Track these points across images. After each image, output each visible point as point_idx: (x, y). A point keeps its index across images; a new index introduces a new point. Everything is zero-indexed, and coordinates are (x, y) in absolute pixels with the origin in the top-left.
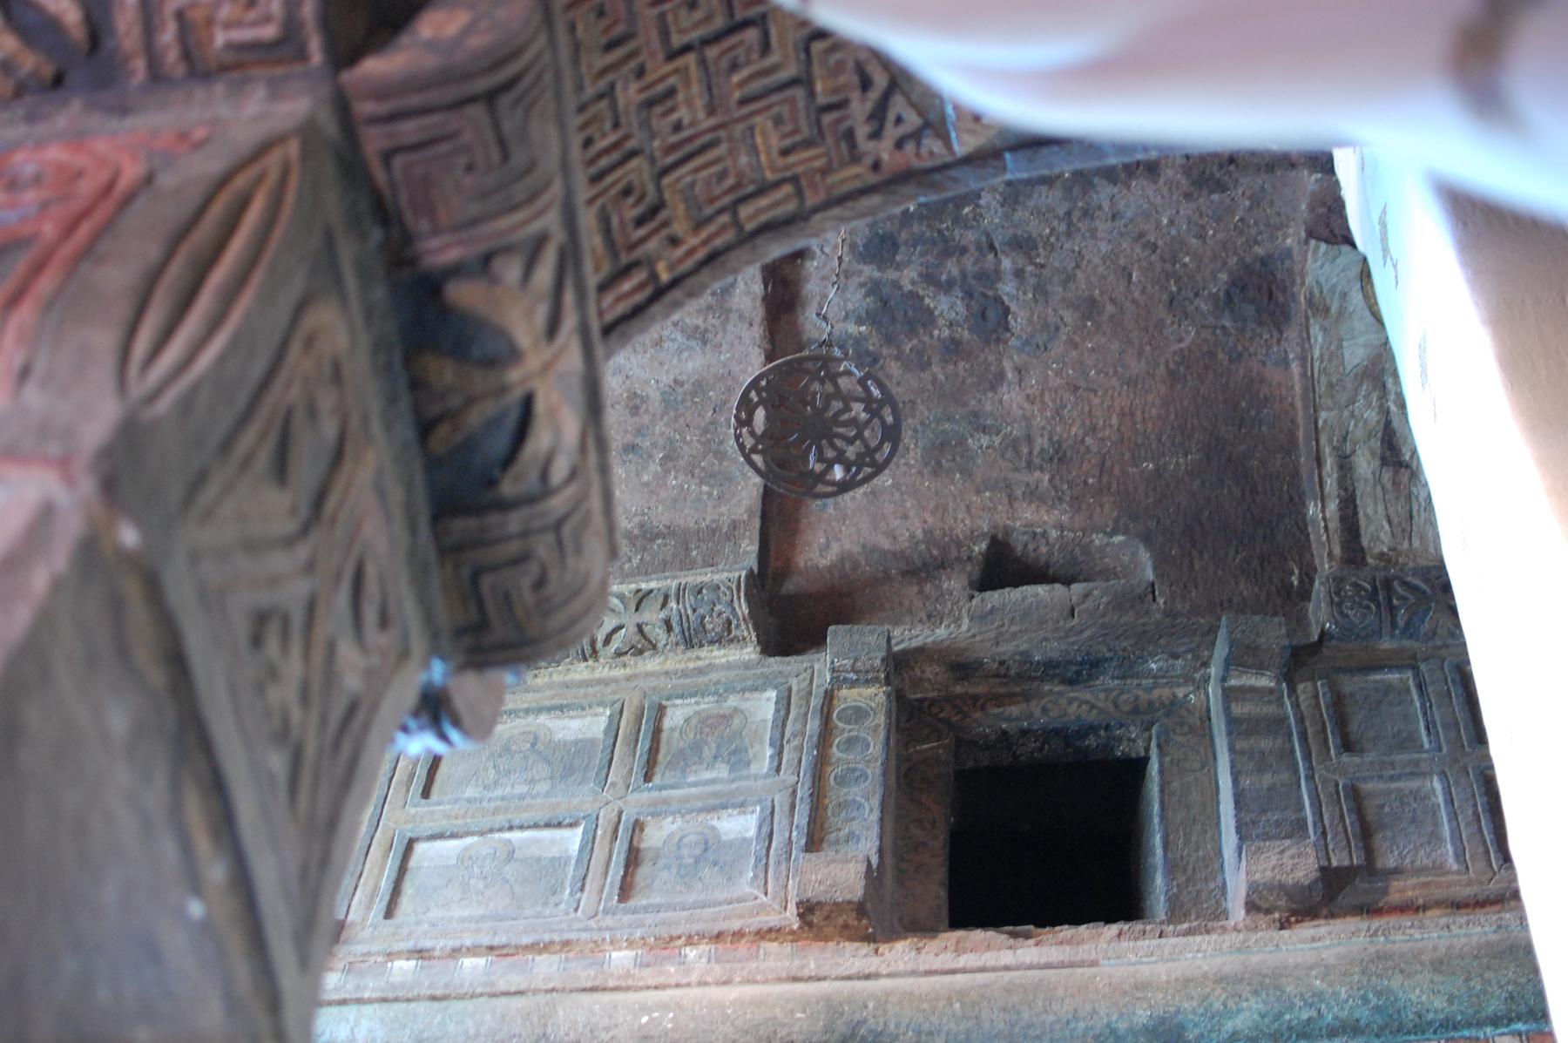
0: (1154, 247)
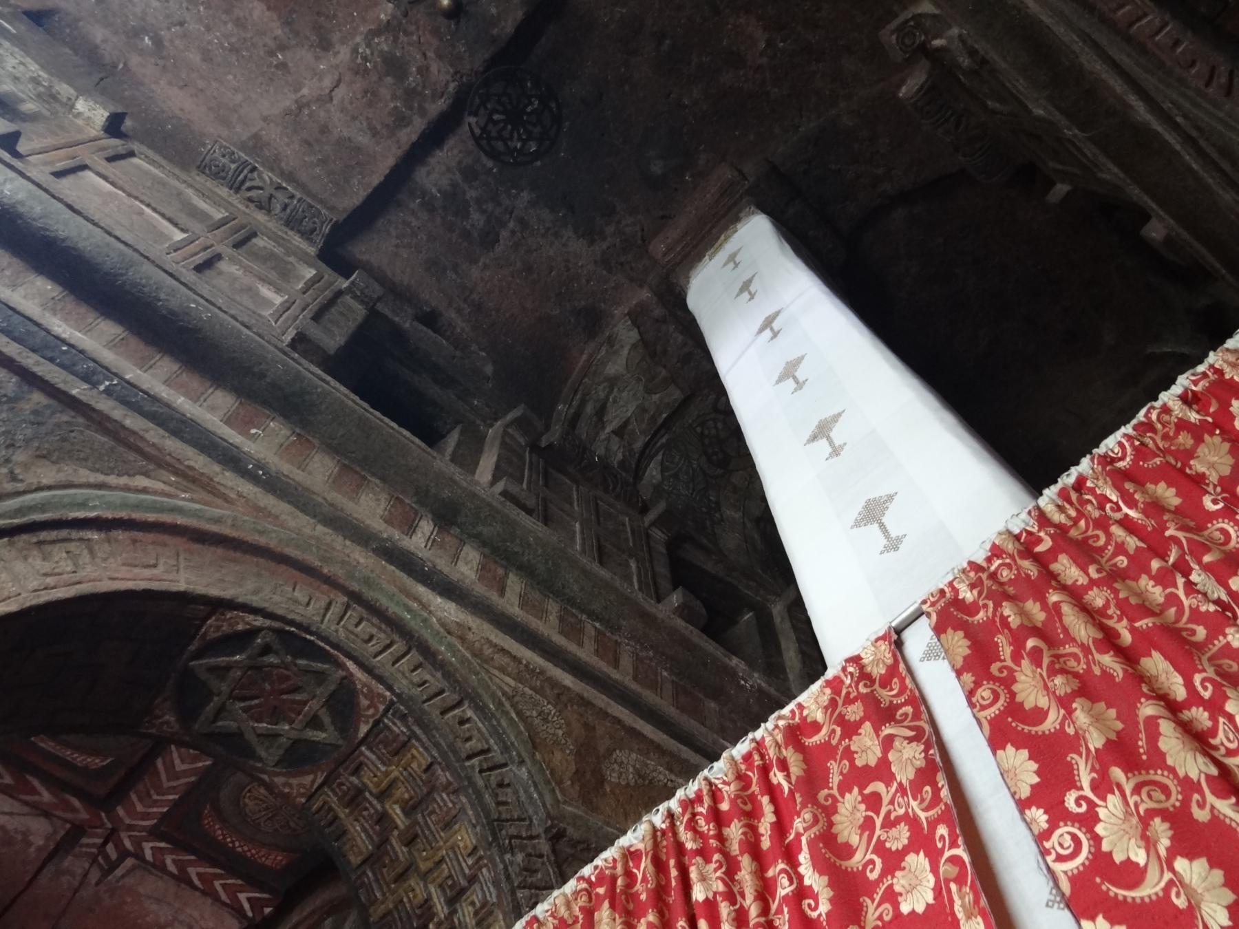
0: (568, 270)
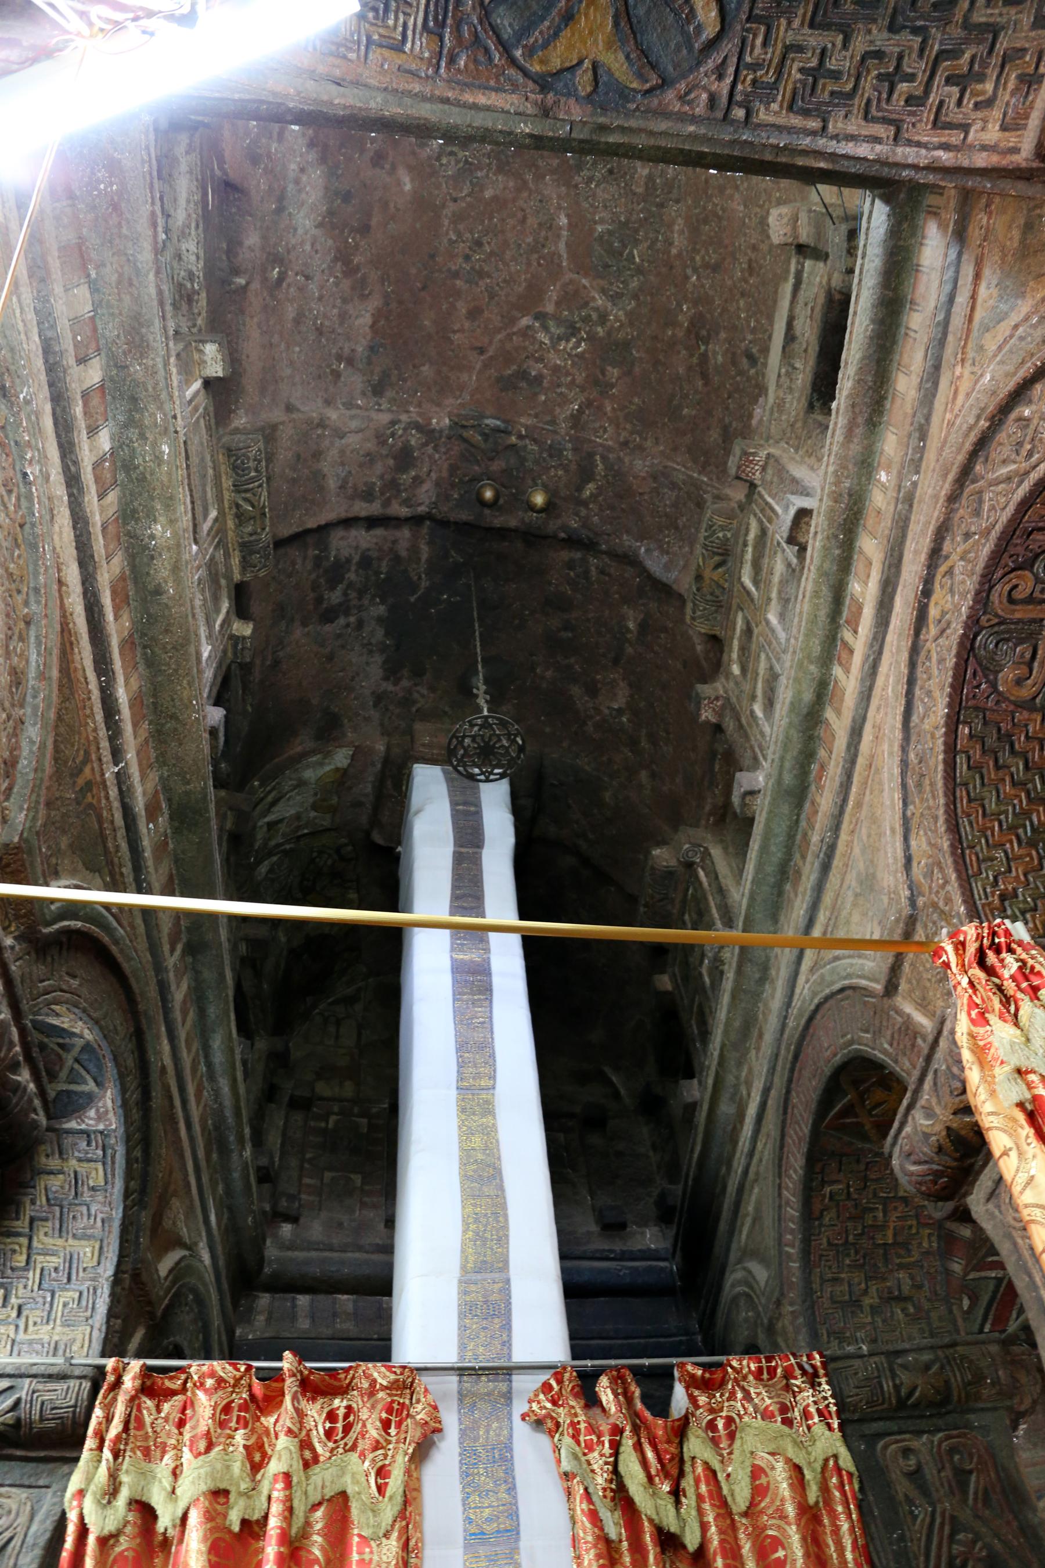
0: (353, 679)
